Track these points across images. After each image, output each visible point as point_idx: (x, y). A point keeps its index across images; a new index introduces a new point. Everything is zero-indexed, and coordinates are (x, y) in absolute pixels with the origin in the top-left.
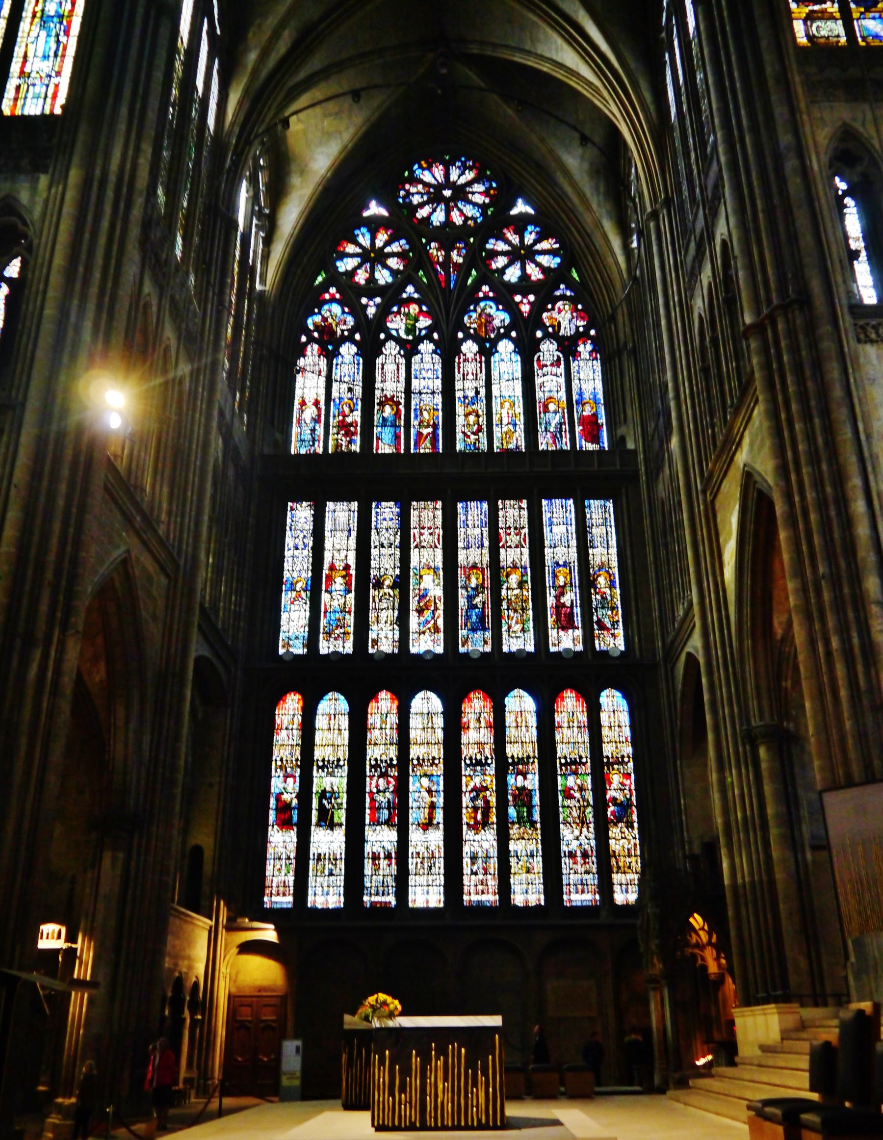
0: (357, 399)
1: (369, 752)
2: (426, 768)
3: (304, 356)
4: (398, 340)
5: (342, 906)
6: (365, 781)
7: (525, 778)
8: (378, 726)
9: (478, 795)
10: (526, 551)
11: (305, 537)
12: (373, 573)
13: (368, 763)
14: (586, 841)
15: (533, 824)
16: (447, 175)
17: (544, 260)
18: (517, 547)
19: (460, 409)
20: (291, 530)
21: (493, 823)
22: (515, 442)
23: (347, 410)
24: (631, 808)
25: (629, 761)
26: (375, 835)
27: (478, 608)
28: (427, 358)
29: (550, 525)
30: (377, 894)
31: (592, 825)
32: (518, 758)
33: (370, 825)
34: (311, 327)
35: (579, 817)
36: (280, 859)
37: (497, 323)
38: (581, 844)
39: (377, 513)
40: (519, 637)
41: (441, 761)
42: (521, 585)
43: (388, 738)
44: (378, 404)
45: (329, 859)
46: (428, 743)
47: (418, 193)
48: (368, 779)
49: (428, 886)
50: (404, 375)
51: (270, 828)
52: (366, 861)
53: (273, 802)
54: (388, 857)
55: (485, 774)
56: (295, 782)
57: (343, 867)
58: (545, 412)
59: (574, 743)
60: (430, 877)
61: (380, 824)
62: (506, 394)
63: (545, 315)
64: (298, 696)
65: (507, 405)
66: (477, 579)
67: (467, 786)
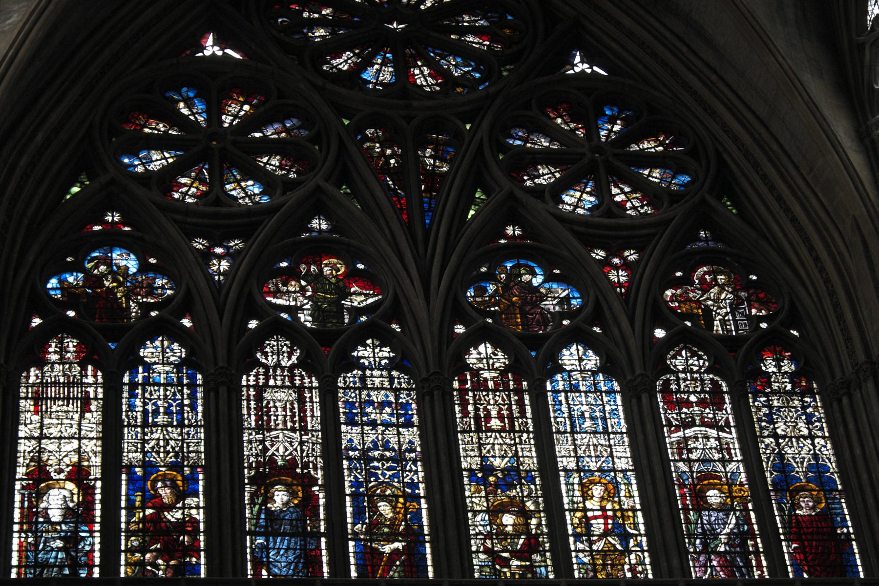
0: (193, 467)
23: (165, 493)
28: (377, 378)
37: (550, 305)
44: (252, 481)
47: (322, 22)
50: (318, 413)
58: (698, 509)
63: (669, 293)
65: (597, 491)
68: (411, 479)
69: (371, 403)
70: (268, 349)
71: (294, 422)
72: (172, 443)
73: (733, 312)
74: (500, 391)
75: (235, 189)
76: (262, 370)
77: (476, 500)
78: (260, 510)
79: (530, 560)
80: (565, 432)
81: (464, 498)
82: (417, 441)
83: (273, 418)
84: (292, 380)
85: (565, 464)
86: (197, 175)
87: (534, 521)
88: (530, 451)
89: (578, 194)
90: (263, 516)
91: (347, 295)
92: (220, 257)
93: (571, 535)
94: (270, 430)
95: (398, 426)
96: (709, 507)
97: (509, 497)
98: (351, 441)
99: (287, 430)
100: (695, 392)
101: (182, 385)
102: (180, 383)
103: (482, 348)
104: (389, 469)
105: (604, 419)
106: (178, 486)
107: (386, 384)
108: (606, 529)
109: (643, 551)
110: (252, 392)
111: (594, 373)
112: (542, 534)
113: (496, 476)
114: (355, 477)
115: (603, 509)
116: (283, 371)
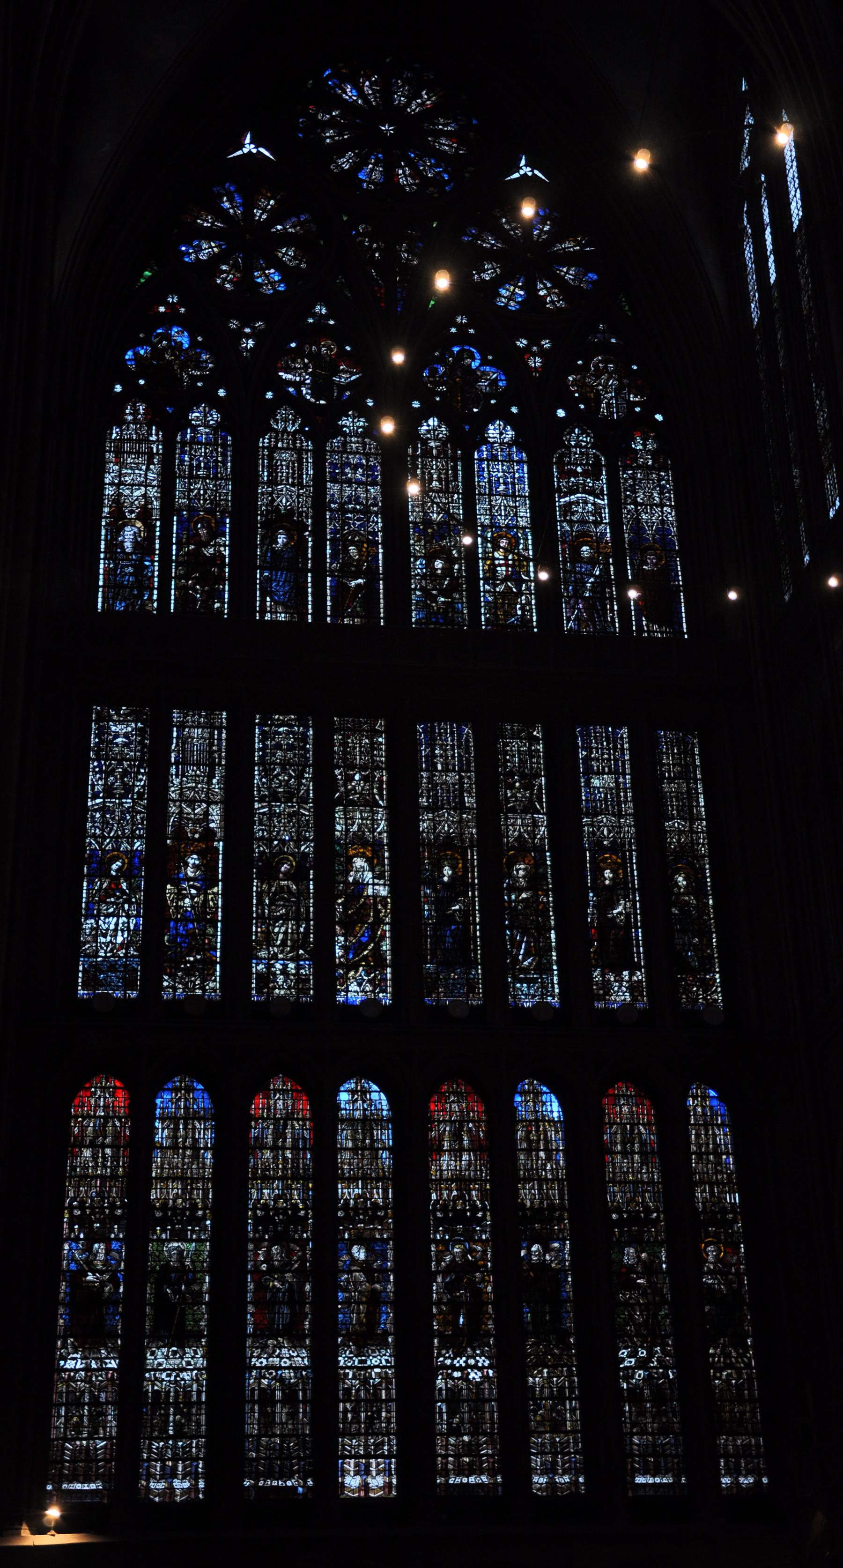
0: (223, 513)
3: (121, 422)
4: (298, 404)
6: (247, 1250)
7: (547, 1249)
8: (270, 1140)
10: (542, 818)
11: (125, 773)
12: (259, 849)
16: (386, 92)
17: (569, 274)
18: (525, 811)
19: (417, 547)
20: (98, 759)
21: (488, 1334)
22: (519, 612)
27: (455, 923)
29: (589, 772)
30: (270, 1475)
33: (253, 1335)
34: (132, 366)
39: (262, 733)
40: (534, 981)
42: (535, 880)
45: (176, 1404)
48: (251, 1246)
49: (367, 1456)
50: (311, 472)
52: (248, 1408)
54: (290, 1399)
55: (471, 1240)
56: (108, 1251)
59: (635, 1183)
62: (502, 522)
65: (503, 543)
66: (453, 868)
67: (438, 1263)
68: (373, 528)
69: (348, 464)
70: (278, 417)
71: (294, 479)
72: (209, 492)
73: (616, 397)
74: (441, 458)
75: (260, 276)
76: (273, 435)
77: (417, 548)
78: (267, 548)
79: (451, 597)
80: (485, 494)
81: (410, 545)
82: (379, 498)
83: (280, 474)
84: (294, 443)
85: (483, 520)
86: (234, 262)
87: (456, 567)
88: (459, 509)
89: (512, 288)
90: (269, 554)
91: (337, 372)
92: (248, 337)
93: (482, 579)
94: (277, 485)
95: (366, 484)
96: (581, 560)
97: (440, 545)
98: (333, 495)
99: (288, 484)
100: (581, 464)
101: (218, 445)
102: (216, 443)
103: (431, 422)
104: (358, 520)
105: (513, 484)
106: (212, 527)
107: (361, 450)
108: (507, 575)
109: (531, 594)
110: (266, 452)
111: (510, 446)
112: (462, 577)
113: (432, 528)
114: (334, 525)
115: (506, 559)
116: (288, 436)
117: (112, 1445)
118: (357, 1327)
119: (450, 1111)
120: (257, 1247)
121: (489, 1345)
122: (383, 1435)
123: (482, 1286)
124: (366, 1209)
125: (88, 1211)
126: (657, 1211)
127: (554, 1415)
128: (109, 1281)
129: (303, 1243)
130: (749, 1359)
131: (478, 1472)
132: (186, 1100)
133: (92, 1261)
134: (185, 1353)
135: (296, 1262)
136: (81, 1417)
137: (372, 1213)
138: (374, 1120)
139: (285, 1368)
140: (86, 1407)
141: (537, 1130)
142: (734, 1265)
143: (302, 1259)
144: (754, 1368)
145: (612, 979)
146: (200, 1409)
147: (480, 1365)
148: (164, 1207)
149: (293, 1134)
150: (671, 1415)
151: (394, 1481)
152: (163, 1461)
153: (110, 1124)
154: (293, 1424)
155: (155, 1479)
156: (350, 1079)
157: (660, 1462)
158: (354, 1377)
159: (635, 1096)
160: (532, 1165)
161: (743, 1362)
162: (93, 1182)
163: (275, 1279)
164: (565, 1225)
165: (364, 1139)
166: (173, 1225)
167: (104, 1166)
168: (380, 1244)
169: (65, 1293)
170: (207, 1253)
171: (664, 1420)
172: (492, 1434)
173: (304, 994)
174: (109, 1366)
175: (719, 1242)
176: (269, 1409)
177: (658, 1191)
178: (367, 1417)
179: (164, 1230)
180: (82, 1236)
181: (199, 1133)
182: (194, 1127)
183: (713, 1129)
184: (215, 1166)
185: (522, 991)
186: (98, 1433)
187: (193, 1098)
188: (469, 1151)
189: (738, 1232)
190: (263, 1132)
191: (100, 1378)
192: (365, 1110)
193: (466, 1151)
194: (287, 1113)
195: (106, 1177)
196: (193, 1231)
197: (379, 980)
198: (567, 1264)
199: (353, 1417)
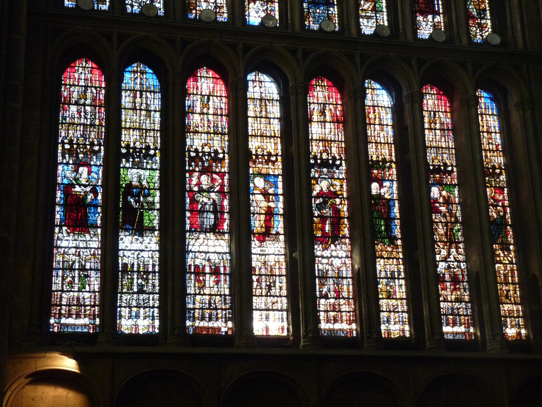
1: (188, 142)
2: (260, 166)
5: (157, 331)
7: (381, 186)
8: (198, 110)
9: (325, 202)
13: (187, 154)
14: (456, 264)
15: (392, 240)
21: (344, 237)
24: (506, 229)
25: (501, 174)
26: (197, 244)
30: (203, 318)
31: (461, 245)
32: (372, 160)
33: (190, 231)
35: (446, 234)
36: (71, 269)
38: (449, 267)
41: (279, 158)
43: (212, 125)
45: (139, 272)
46: (262, 136)
48: (187, 175)
49: (267, 310)
51: (57, 230)
53: (59, 194)
55: (332, 178)
56: (90, 173)
57: (157, 283)
60: (270, 299)
61: (206, 232)
64: (90, 64)
117: (95, 296)
118: (259, 229)
119: (317, 97)
120: (191, 176)
121: (345, 244)
122: (277, 296)
123: (340, 207)
124: (263, 155)
125: (75, 146)
126: (452, 166)
127: (388, 288)
128: (91, 191)
129: (222, 175)
130: (512, 258)
131: (340, 321)
132: (141, 79)
133: (78, 179)
134: (143, 241)
135: (218, 186)
136: (73, 278)
137: (268, 158)
138: (268, 100)
139: (211, 253)
140: (77, 271)
141: (374, 112)
142: (501, 201)
143: (222, 185)
144: (514, 264)
145: (422, 20)
146: (155, 276)
147: (340, 256)
148: (128, 147)
149: (214, 105)
150: (462, 290)
151: (285, 324)
152: (130, 307)
153: (89, 91)
154: (218, 288)
155: (125, 318)
156: (251, 73)
157: (456, 319)
158: (258, 260)
159: (436, 94)
160: (371, 133)
161: (508, 260)
162: (78, 128)
163: (203, 196)
164: (393, 172)
165: (261, 111)
166: (134, 159)
167: (86, 118)
168: (273, 177)
169: (61, 198)
170: (157, 178)
171: (459, 293)
172: (348, 298)
173: (220, 15)
174: (91, 246)
175: (491, 186)
176: (201, 278)
177: (452, 154)
178: (266, 285)
179: (128, 161)
180: (71, 162)
181: (150, 101)
182: (147, 98)
183: (486, 117)
184: (161, 123)
185: (363, 24)
186: (84, 288)
187: (146, 78)
188: (330, 122)
189: (503, 181)
190: (193, 103)
191: (86, 254)
192: (261, 93)
193: (329, 122)
194: (210, 92)
195: (87, 125)
196: (147, 163)
197: (270, 11)
198: (395, 195)
199: (257, 285)
